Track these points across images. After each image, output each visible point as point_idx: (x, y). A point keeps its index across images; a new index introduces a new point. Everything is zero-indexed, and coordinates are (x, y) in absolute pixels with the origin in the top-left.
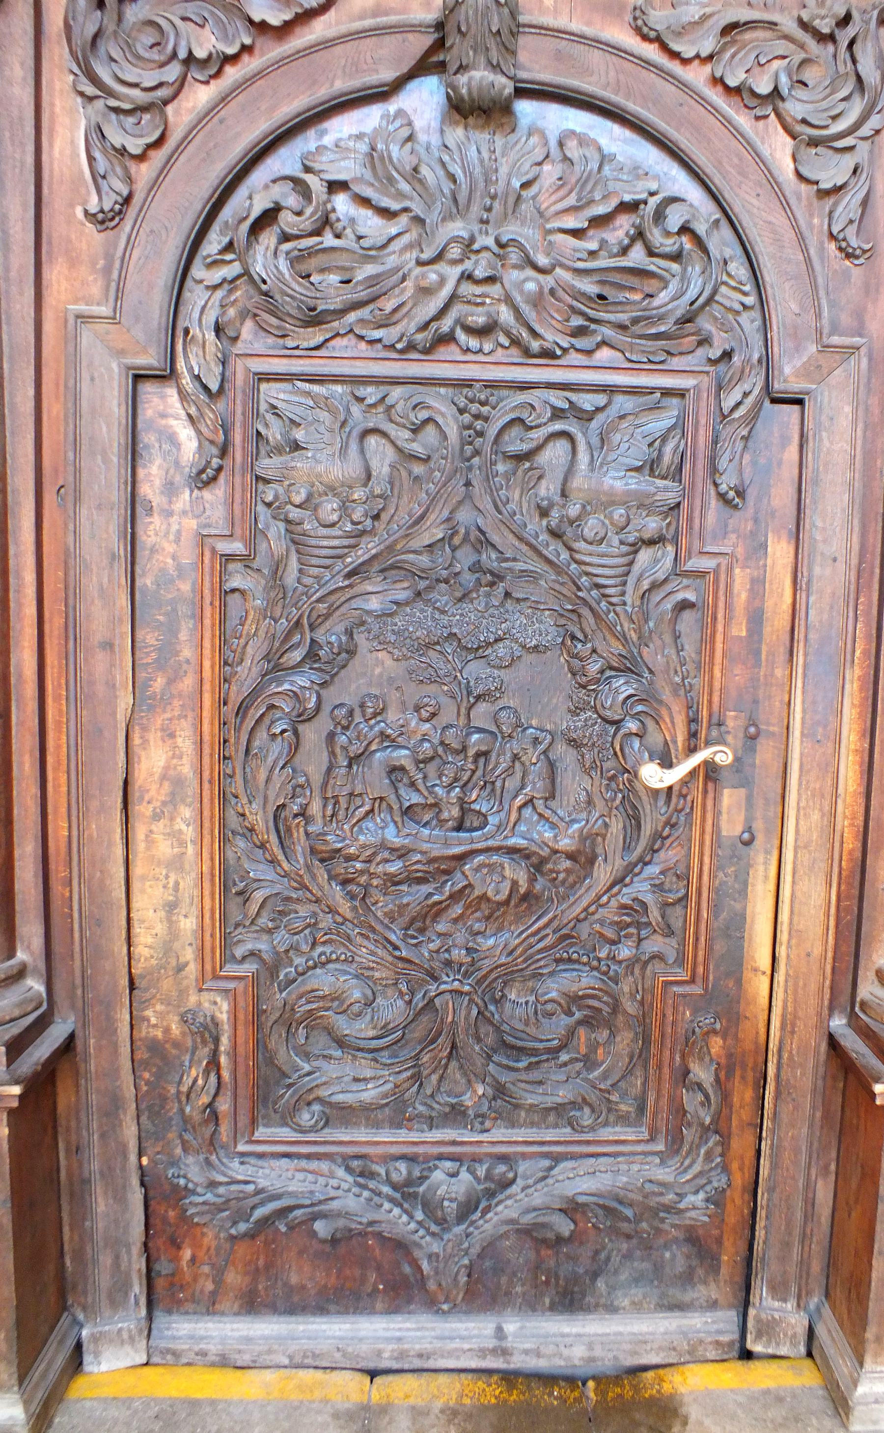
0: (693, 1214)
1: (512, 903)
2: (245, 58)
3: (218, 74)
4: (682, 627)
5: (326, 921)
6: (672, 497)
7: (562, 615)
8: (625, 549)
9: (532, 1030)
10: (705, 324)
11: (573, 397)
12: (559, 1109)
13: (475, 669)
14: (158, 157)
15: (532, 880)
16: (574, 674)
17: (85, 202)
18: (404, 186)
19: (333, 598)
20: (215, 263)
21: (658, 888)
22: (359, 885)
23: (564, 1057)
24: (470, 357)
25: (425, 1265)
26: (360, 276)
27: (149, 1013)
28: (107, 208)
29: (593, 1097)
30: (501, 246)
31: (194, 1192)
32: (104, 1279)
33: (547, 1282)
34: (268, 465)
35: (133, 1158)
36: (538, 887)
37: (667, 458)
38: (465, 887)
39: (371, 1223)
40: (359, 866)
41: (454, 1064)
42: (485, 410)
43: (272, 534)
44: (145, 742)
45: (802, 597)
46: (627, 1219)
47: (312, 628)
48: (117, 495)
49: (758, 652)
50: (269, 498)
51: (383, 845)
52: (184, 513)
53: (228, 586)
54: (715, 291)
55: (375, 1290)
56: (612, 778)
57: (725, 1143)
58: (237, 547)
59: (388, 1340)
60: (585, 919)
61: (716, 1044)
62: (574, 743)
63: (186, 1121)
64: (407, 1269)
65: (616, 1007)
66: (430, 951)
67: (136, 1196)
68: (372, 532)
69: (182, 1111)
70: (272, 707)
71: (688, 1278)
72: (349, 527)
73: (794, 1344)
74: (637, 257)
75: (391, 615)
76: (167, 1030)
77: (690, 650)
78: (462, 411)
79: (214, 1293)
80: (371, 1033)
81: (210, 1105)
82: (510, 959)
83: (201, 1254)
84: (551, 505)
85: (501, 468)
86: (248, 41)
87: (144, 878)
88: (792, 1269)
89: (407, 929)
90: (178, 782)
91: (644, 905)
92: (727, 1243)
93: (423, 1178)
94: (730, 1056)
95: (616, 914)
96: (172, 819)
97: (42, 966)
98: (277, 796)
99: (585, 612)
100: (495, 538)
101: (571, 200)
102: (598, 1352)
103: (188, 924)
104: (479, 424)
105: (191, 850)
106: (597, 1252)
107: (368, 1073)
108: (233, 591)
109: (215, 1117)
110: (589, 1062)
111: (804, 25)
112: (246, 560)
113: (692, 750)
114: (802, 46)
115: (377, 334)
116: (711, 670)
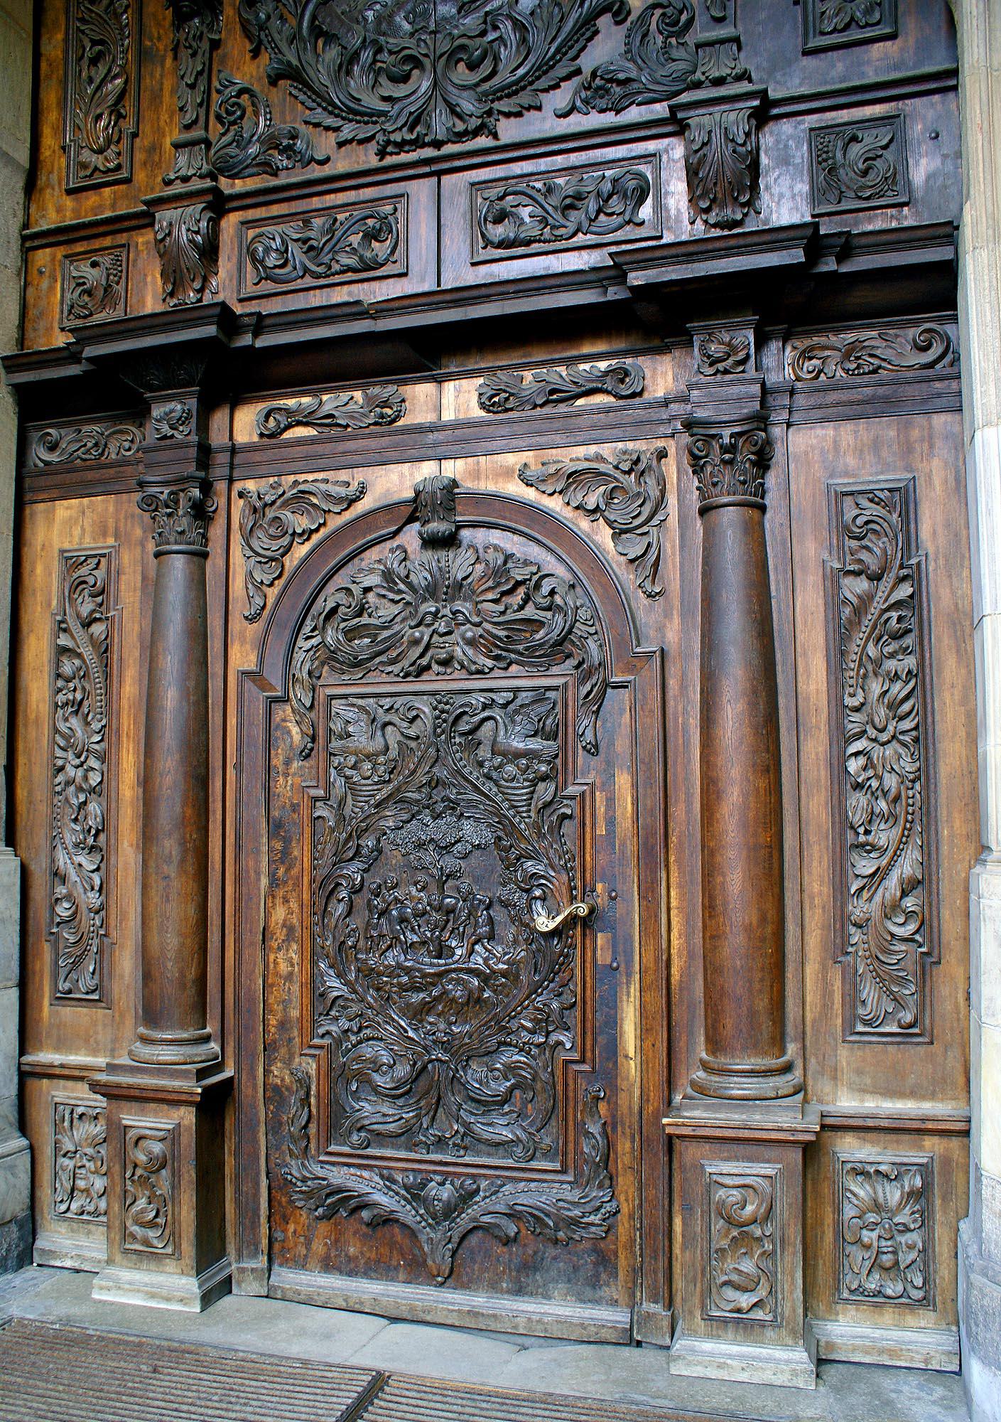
3: (308, 539)
8: (526, 784)
10: (568, 647)
18: (402, 586)
23: (507, 1108)
24: (440, 677)
30: (454, 613)
33: (504, 1272)
43: (338, 783)
53: (316, 815)
54: (572, 627)
58: (321, 793)
63: (292, 1136)
68: (389, 781)
76: (283, 1080)
80: (393, 1085)
101: (490, 583)
104: (444, 716)
108: (319, 817)
111: (616, 468)
112: (325, 799)
115: (390, 669)
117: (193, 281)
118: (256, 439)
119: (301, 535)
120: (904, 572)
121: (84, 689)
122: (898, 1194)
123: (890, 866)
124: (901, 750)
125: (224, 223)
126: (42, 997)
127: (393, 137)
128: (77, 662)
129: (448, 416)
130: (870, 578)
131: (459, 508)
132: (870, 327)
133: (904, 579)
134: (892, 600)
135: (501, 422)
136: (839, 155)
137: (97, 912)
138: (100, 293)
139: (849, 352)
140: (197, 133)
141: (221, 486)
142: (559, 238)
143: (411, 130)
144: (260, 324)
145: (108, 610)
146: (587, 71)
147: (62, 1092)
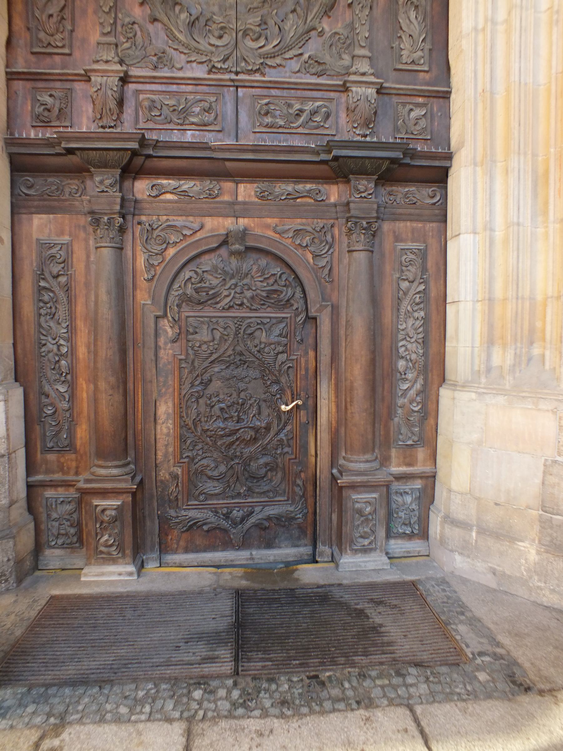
0: (299, 520)
4: (289, 372)
5: (206, 447)
6: (285, 342)
10: (292, 302)
12: (264, 493)
15: (256, 435)
20: (177, 291)
21: (286, 435)
26: (210, 293)
32: (148, 543)
34: (190, 337)
44: (160, 405)
47: (202, 375)
48: (153, 345)
49: (307, 378)
51: (219, 427)
52: (169, 349)
57: (306, 500)
58: (183, 357)
61: (303, 475)
62: (265, 401)
64: (227, 539)
67: (157, 522)
68: (216, 353)
71: (299, 538)
74: (275, 287)
76: (165, 477)
77: (291, 378)
79: (177, 548)
85: (245, 336)
90: (168, 414)
92: (309, 528)
93: (231, 512)
100: (245, 353)
102: (277, 558)
103: (171, 450)
105: (171, 431)
110: (271, 480)
111: (314, 229)
113: (293, 402)
117: (112, 115)
118: (145, 197)
120: (422, 280)
121: (56, 308)
122: (410, 499)
123: (413, 386)
124: (419, 346)
125: (125, 88)
126: (37, 451)
127: (216, 65)
128: (51, 295)
129: (240, 199)
130: (409, 282)
131: (247, 240)
132: (414, 186)
133: (420, 283)
134: (418, 290)
135: (265, 205)
136: (406, 116)
137: (67, 411)
138: (56, 110)
139: (406, 196)
140: (111, 39)
141: (129, 217)
142: (293, 128)
143: (224, 63)
144: (157, 144)
145: (68, 271)
146: (306, 56)
147: (49, 493)
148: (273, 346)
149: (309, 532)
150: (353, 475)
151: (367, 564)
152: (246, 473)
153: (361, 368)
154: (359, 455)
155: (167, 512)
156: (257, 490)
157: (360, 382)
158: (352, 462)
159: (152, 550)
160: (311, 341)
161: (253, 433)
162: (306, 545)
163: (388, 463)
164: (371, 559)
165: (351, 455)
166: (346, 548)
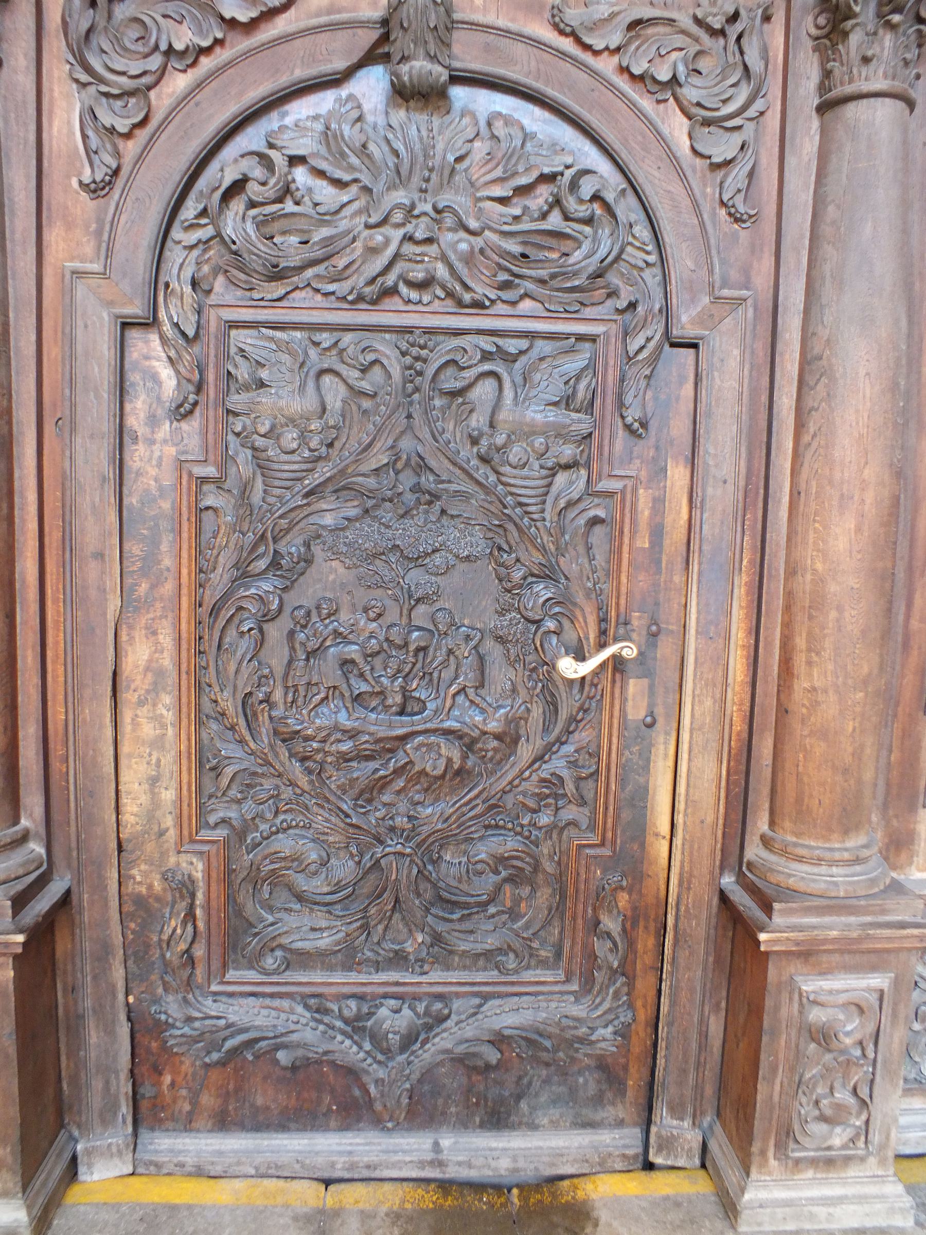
0: (603, 1045)
1: (448, 777)
2: (218, 50)
3: (194, 64)
5: (287, 793)
6: (585, 428)
7: (490, 530)
8: (544, 472)
9: (464, 887)
10: (613, 279)
11: (500, 341)
12: (488, 955)
13: (415, 576)
14: (143, 135)
15: (465, 757)
16: (500, 580)
17: (80, 174)
18: (354, 160)
19: (293, 515)
20: (192, 227)
21: (573, 764)
22: (315, 762)
23: (492, 910)
24: (411, 307)
25: (372, 1089)
26: (316, 237)
27: (135, 872)
28: (98, 179)
29: (517, 944)
30: (438, 211)
31: (173, 1026)
32: (95, 1099)
34: (237, 400)
35: (121, 996)
36: (470, 763)
37: (580, 394)
38: (407, 764)
39: (326, 1053)
40: (315, 745)
41: (397, 916)
42: (424, 353)
43: (240, 459)
44: (131, 639)
45: (697, 514)
46: (546, 1049)
47: (275, 539)
48: (107, 426)
49: (658, 562)
50: (238, 429)
51: (336, 727)
52: (165, 441)
53: (202, 505)
54: (622, 251)
55: (330, 1110)
56: (534, 670)
57: (631, 984)
58: (210, 471)
59: (340, 1153)
60: (510, 791)
61: (623, 899)
62: (500, 640)
63: (166, 964)
64: (357, 1092)
65: (536, 866)
66: (377, 819)
67: (124, 1030)
68: (326, 458)
69: (163, 956)
70: (240, 608)
71: (598, 1100)
72: (307, 454)
73: (690, 1157)
75: (343, 529)
76: (150, 887)
78: (404, 354)
79: (190, 1113)
80: (326, 889)
81: (187, 951)
82: (445, 825)
83: (179, 1079)
84: (481, 435)
85: (438, 402)
86: (219, 35)
87: (130, 756)
88: (688, 1092)
89: (356, 799)
90: (160, 673)
91: (561, 779)
92: (633, 1070)
93: (371, 1014)
94: (634, 909)
95: (537, 787)
96: (155, 705)
97: (42, 831)
98: (245, 685)
99: (510, 527)
100: (433, 463)
101: (498, 173)
102: (521, 1164)
103: (168, 795)
104: (418, 366)
105: (170, 731)
106: (520, 1078)
107: (324, 924)
108: (207, 508)
109: (191, 961)
110: (514, 914)
112: (218, 482)
113: (602, 646)
114: (697, 40)
115: (331, 287)
116: (619, 577)
119: (183, 54)
148: (539, 441)
149: (634, 1081)
150: (808, 911)
151: (837, 1211)
152: (423, 885)
153: (858, 529)
154: (827, 839)
155: (156, 1001)
156: (464, 946)
157: (853, 581)
158: (800, 859)
159: (107, 1117)
160: (680, 428)
161: (456, 755)
162: (620, 1123)
163: (904, 856)
164: (850, 1191)
165: (797, 835)
166: (763, 1153)
